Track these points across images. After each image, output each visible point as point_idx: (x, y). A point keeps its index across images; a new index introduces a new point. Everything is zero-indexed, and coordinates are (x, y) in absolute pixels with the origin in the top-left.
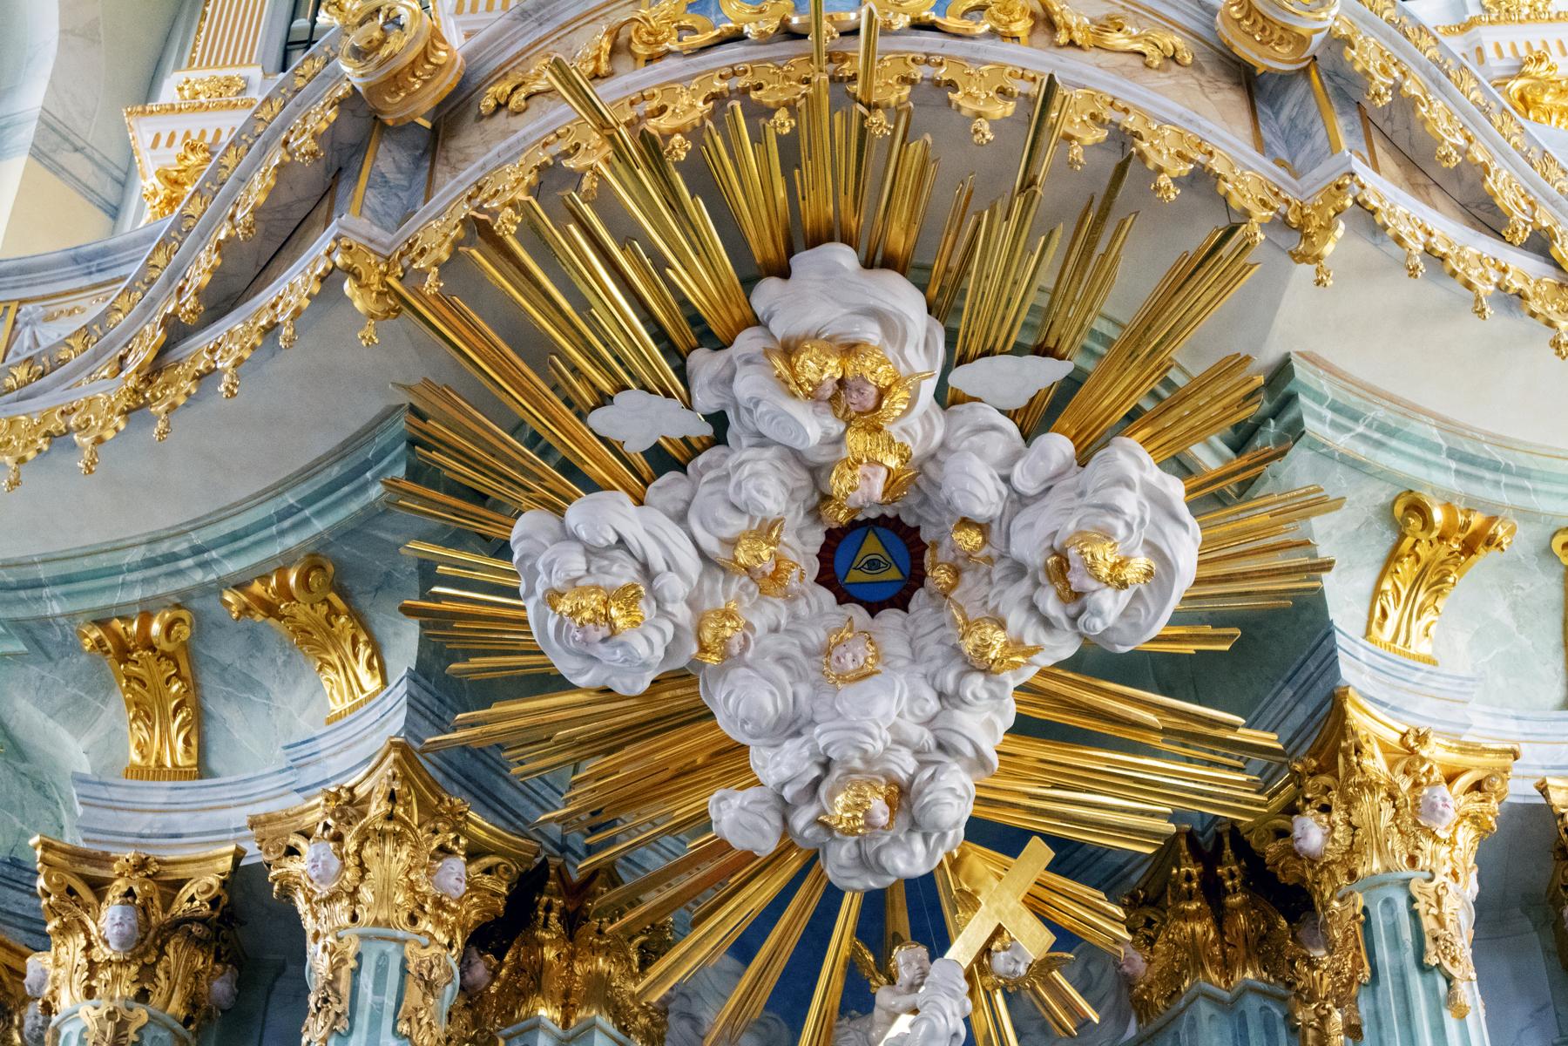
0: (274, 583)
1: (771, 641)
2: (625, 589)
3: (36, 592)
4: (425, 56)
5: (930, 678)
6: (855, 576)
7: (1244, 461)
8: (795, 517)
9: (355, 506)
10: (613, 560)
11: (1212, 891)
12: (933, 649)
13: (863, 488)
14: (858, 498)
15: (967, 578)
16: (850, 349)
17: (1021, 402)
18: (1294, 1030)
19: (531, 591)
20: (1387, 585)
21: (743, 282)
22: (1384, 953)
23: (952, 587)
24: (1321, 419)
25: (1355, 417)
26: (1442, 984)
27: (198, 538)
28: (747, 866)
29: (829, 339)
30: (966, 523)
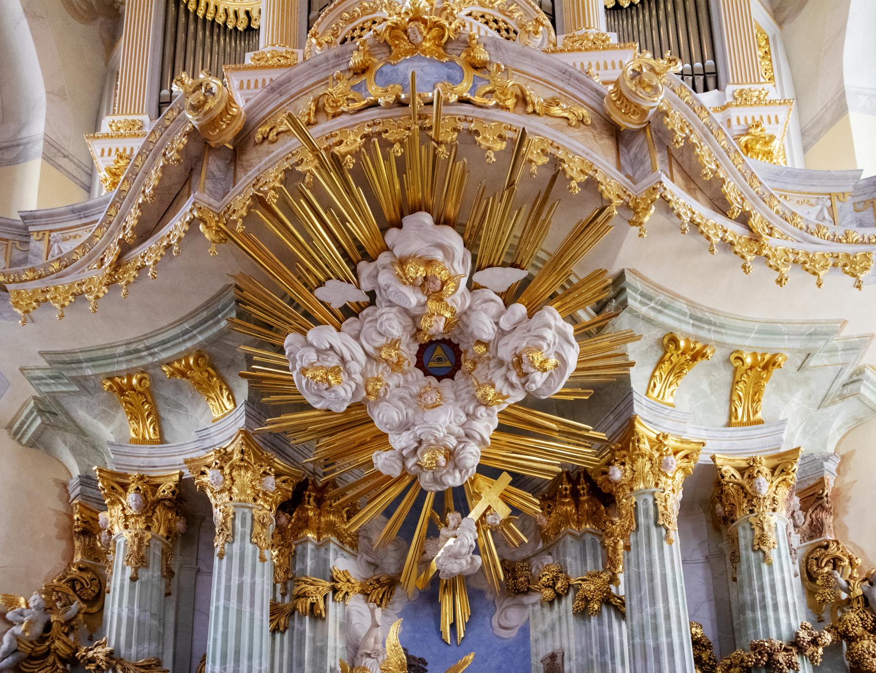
0: (183, 363)
1: (397, 391)
2: (334, 368)
3: (79, 365)
4: (226, 110)
5: (463, 408)
6: (432, 364)
7: (600, 318)
8: (406, 338)
9: (215, 330)
10: (328, 356)
11: (575, 494)
12: (464, 395)
13: (436, 326)
14: (433, 330)
15: (479, 366)
16: (429, 263)
17: (505, 289)
18: (604, 547)
19: (294, 368)
20: (657, 373)
21: (381, 230)
22: (642, 520)
23: (473, 370)
24: (635, 299)
25: (651, 299)
26: (664, 531)
27: (148, 343)
28: (388, 481)
29: (420, 258)
30: (479, 342)
